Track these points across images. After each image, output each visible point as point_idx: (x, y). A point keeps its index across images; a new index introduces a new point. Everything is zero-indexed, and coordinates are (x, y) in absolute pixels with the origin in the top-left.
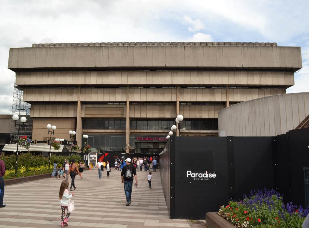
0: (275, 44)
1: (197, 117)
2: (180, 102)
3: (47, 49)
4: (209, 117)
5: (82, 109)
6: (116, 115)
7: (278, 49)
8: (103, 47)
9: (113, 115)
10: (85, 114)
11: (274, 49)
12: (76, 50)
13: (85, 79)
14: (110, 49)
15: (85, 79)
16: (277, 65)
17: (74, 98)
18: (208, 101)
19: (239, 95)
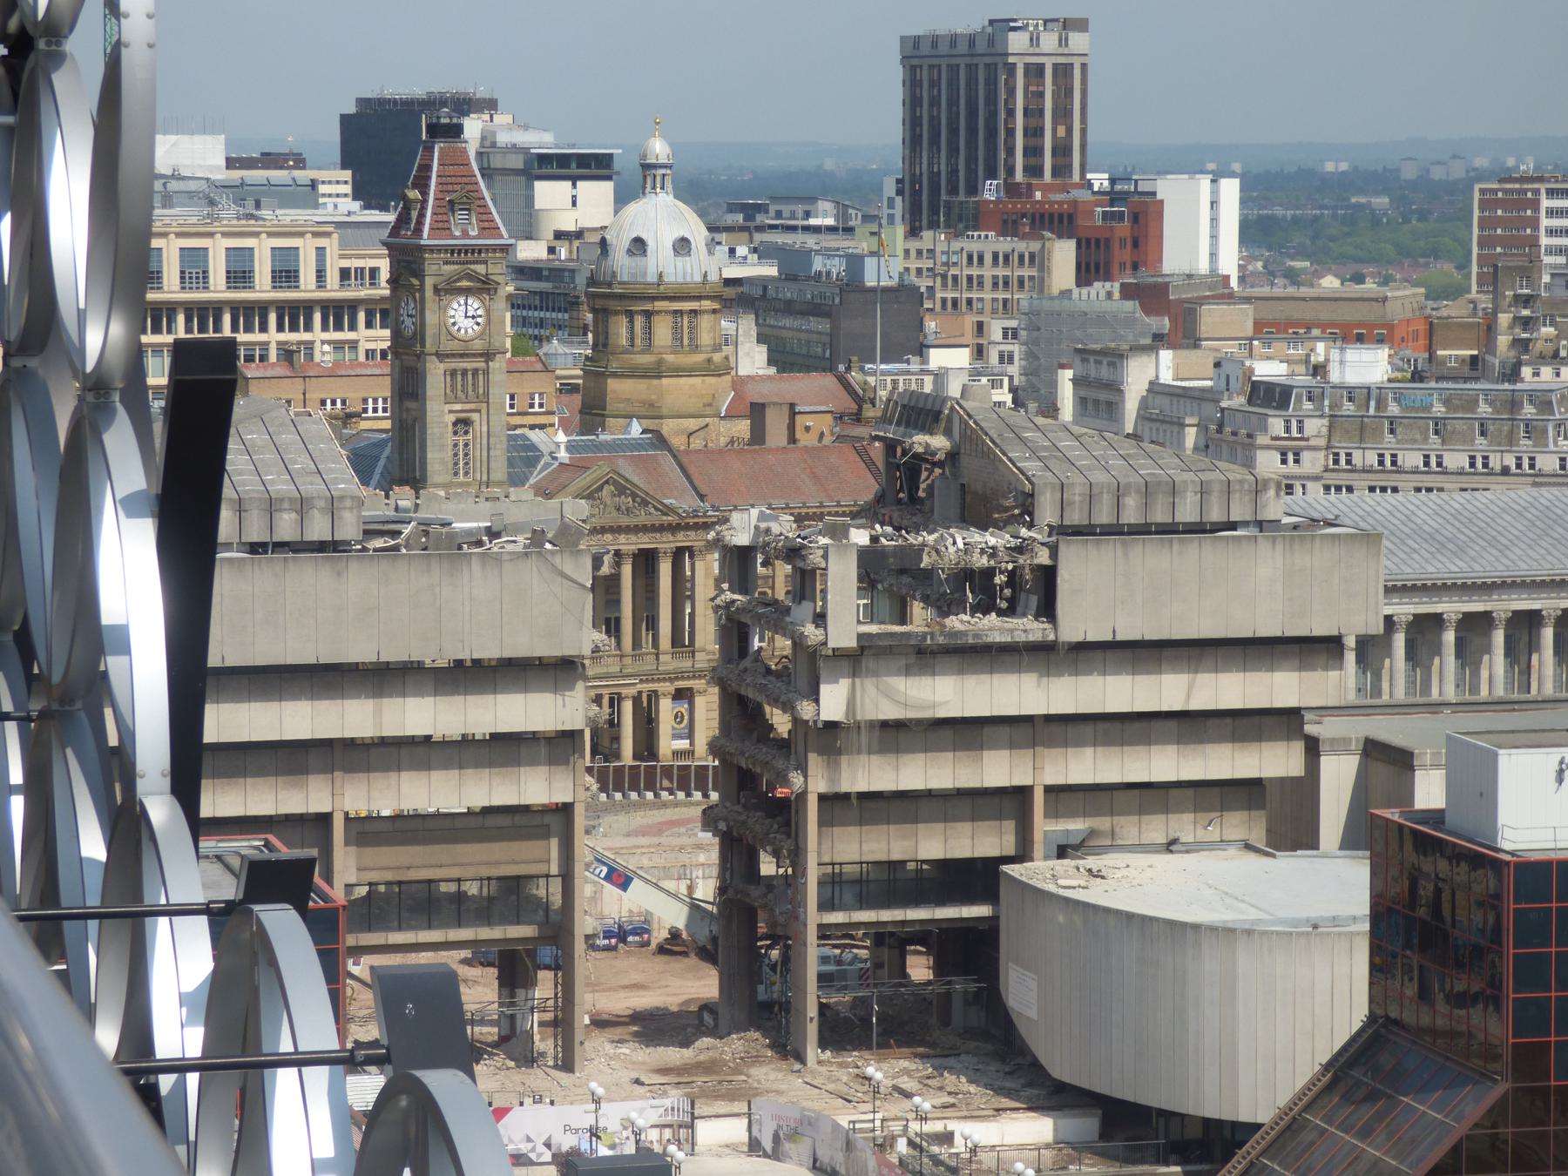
5: (347, 843)
7: (1279, 547)
8: (476, 565)
9: (498, 863)
10: (359, 869)
12: (339, 574)
13: (378, 713)
14: (507, 567)
15: (378, 713)
16: (1268, 628)
17: (312, 795)
18: (949, 785)
19: (1089, 751)
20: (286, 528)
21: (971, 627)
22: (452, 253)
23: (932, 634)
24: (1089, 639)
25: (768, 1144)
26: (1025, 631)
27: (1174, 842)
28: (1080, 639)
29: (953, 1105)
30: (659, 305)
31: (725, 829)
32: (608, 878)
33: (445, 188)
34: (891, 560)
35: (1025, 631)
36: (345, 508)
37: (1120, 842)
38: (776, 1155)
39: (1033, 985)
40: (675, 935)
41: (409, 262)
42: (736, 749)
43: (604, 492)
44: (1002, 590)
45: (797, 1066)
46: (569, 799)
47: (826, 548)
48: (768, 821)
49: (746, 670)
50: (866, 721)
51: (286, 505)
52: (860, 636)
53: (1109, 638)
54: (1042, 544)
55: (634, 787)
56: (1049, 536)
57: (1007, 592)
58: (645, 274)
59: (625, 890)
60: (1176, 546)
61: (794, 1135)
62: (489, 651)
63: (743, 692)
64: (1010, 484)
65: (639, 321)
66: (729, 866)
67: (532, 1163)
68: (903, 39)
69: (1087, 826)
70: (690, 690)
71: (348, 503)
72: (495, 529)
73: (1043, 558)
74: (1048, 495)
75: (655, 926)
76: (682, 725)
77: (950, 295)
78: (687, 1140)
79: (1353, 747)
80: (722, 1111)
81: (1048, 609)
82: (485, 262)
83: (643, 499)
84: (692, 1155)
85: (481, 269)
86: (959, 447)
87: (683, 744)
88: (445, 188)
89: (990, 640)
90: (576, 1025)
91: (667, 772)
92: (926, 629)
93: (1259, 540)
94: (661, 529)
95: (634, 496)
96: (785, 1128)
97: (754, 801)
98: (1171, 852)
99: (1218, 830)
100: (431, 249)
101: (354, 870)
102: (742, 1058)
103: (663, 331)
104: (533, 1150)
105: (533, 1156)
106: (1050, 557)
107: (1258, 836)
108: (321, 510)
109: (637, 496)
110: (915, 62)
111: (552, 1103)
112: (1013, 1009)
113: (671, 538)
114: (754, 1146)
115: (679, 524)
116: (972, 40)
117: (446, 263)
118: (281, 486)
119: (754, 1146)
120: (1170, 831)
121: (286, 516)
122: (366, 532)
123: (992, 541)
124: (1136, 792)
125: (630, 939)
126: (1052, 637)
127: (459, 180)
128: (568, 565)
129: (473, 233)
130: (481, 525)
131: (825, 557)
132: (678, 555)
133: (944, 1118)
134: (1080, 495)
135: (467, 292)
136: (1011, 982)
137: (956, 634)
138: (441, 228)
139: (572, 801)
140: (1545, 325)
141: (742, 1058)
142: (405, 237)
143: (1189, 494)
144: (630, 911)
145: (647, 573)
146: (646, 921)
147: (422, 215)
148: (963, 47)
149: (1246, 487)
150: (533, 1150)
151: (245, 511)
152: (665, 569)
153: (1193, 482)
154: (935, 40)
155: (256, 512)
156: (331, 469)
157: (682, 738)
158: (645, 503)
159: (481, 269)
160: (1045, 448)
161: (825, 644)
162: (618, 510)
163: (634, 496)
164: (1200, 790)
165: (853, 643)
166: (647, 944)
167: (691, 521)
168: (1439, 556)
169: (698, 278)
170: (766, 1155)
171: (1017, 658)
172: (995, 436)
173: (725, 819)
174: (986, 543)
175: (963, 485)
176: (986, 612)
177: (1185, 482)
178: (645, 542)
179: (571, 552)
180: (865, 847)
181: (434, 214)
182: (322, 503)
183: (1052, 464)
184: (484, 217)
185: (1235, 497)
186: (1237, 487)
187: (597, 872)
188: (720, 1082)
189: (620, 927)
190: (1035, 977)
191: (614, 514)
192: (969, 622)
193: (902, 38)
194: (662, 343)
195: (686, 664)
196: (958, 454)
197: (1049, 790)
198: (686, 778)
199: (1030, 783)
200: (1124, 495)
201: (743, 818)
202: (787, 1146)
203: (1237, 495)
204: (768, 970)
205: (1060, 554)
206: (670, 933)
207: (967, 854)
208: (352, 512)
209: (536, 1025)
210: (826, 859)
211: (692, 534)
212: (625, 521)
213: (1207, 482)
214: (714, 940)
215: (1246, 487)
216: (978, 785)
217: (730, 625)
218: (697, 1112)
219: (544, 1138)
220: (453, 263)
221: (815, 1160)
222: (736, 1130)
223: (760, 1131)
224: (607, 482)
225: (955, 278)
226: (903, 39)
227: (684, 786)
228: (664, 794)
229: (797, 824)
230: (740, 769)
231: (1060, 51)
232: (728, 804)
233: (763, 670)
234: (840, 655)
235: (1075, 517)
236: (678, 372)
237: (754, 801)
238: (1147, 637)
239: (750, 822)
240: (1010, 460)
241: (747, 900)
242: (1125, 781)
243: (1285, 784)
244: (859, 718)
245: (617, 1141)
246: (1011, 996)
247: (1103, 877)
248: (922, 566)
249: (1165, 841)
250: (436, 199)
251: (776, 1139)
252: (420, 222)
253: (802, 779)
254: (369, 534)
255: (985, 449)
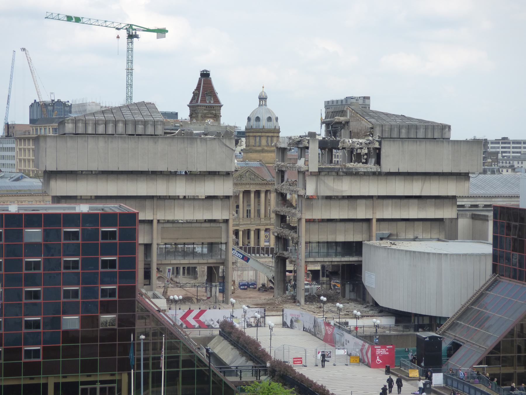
0: (447, 127)
1: (329, 240)
2: (308, 221)
3: (106, 139)
4: (346, 240)
6: (211, 238)
7: (450, 144)
8: (198, 140)
10: (162, 239)
11: (445, 144)
12: (155, 143)
14: (208, 142)
16: (446, 170)
20: (140, 129)
21: (354, 167)
22: (206, 108)
23: (342, 168)
24: (391, 171)
25: (289, 324)
26: (371, 168)
27: (417, 238)
28: (388, 171)
29: (348, 315)
30: (263, 134)
31: (277, 235)
32: (242, 258)
33: (205, 90)
34: (329, 144)
35: (371, 168)
36: (159, 124)
37: (399, 238)
38: (292, 327)
39: (373, 277)
40: (263, 285)
41: (195, 110)
42: (280, 210)
43: (247, 174)
44: (363, 156)
45: (298, 304)
46: (227, 218)
47: (308, 140)
48: (290, 231)
49: (283, 185)
50: (321, 196)
51: (140, 123)
52: (319, 168)
53: (397, 171)
54: (377, 141)
55: (254, 253)
56: (379, 139)
57: (365, 157)
58: (259, 126)
59: (248, 262)
60: (418, 143)
61: (297, 321)
62: (204, 169)
63: (282, 192)
64: (366, 126)
65: (258, 139)
66: (278, 246)
67: (212, 328)
68: (325, 102)
69: (389, 232)
70: (269, 229)
71: (159, 123)
72: (205, 133)
73: (377, 145)
74: (378, 128)
75: (258, 284)
76: (267, 239)
77: (336, 160)
78: (263, 322)
79: (468, 216)
80: (274, 314)
81: (378, 162)
82: (215, 110)
83: (257, 176)
84: (264, 327)
85: (214, 112)
86: (349, 120)
87: (267, 244)
88: (205, 90)
89: (360, 171)
90: (229, 289)
91: (263, 249)
92: (340, 167)
93: (444, 142)
94: (262, 184)
95: (255, 175)
96: (294, 318)
97: (285, 226)
98: (415, 241)
99: (430, 235)
100: (201, 106)
101: (160, 239)
102: (281, 302)
103: (264, 142)
104: (213, 324)
105: (213, 326)
106: (379, 145)
107: (442, 237)
108: (151, 125)
109: (255, 175)
110: (328, 107)
111: (220, 309)
112: (367, 286)
113: (265, 187)
114: (284, 324)
115: (267, 184)
116: (342, 101)
117: (205, 110)
118: (139, 118)
119: (284, 324)
120: (415, 235)
121: (140, 126)
122: (165, 133)
123: (361, 141)
124: (404, 223)
125: (251, 286)
126: (379, 170)
127: (208, 88)
128: (227, 143)
129: (212, 102)
130: (201, 132)
131: (308, 143)
132: (267, 192)
133: (345, 318)
134: (388, 128)
135: (210, 117)
136: (366, 278)
137: (349, 168)
138: (204, 100)
139: (228, 219)
140: (489, 159)
141: (281, 302)
142: (194, 103)
143: (421, 129)
144: (251, 279)
145: (258, 198)
146: (255, 282)
147: (199, 97)
148: (340, 103)
149: (439, 127)
150: (213, 324)
151: (127, 124)
152: (263, 196)
153: (423, 125)
154: (333, 101)
155: (131, 124)
156: (153, 111)
157: (267, 242)
158: (258, 177)
159: (214, 112)
160: (377, 117)
161: (308, 171)
162: (250, 179)
163: (255, 175)
164: (425, 222)
165: (317, 171)
166: (256, 288)
167: (270, 183)
168: (477, 189)
169: (273, 128)
170: (288, 327)
171: (368, 177)
172: (361, 114)
173: (276, 232)
174: (359, 142)
175: (351, 131)
176: (359, 163)
177: (421, 125)
178: (258, 189)
179: (229, 138)
180: (320, 237)
181: (201, 97)
182: (151, 123)
183: (378, 120)
184: (215, 98)
185: (436, 131)
186: (437, 127)
187: (239, 257)
188: (274, 307)
189: (248, 283)
190: (374, 274)
191: (249, 180)
192: (353, 165)
193: (325, 102)
194: (264, 144)
195: (268, 222)
196: (349, 122)
197: (379, 220)
198: (267, 251)
199: (372, 218)
200: (401, 129)
201: (282, 231)
202: (295, 324)
203: (437, 130)
204: (290, 287)
205: (382, 144)
206: (262, 285)
207: (352, 240)
208: (161, 126)
209: (218, 292)
210: (308, 240)
211: (270, 186)
212: (252, 182)
213: (427, 125)
214: (273, 278)
215: (439, 127)
216: (355, 218)
217: (279, 172)
218: (266, 314)
219: (217, 320)
220: (207, 110)
221: (304, 328)
222: (279, 319)
223: (286, 319)
224: (247, 171)
225: (338, 155)
226: (325, 102)
227: (267, 253)
228: (262, 255)
229: (299, 229)
230: (281, 215)
231: (363, 104)
232: (278, 228)
233: (289, 184)
234: (312, 174)
235: (386, 135)
236: (267, 151)
237: (285, 226)
238: (409, 171)
239: (284, 232)
240: (366, 119)
241: (283, 256)
242: (401, 218)
243: (451, 220)
244: (319, 195)
245: (240, 321)
246: (366, 282)
247: (395, 245)
248: (339, 146)
249: (413, 238)
250: (202, 93)
251: (292, 321)
252: (198, 99)
253: (300, 214)
254: (165, 133)
255: (358, 118)
